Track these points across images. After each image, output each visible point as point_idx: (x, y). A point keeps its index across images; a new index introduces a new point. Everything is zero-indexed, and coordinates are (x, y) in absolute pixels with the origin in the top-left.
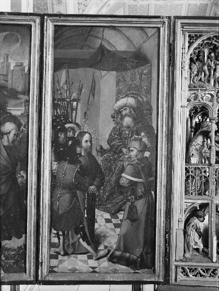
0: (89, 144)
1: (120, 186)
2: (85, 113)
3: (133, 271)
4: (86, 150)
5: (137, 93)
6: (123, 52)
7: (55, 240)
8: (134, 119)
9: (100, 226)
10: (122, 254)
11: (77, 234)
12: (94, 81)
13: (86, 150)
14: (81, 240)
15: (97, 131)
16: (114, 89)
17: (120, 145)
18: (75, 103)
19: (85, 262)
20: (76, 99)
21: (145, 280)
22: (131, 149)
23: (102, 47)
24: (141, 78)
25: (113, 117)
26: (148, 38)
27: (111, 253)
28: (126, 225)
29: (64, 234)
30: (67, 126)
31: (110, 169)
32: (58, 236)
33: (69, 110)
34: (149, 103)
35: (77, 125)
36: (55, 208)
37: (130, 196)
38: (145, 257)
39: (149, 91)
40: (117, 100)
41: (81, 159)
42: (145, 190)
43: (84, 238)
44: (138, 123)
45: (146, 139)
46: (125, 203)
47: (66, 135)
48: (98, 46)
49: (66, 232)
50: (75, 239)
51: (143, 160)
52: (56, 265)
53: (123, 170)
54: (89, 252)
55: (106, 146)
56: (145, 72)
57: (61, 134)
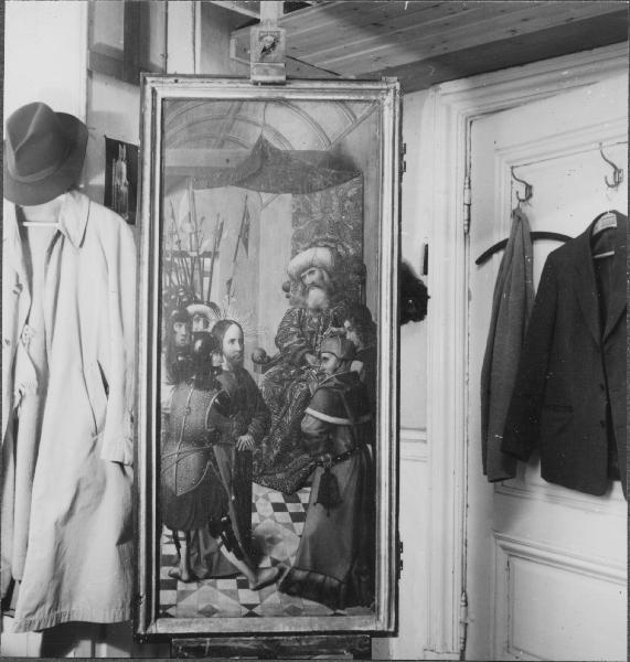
0: (237, 347)
1: (302, 435)
2: (229, 282)
3: (332, 612)
4: (230, 359)
5: (337, 238)
6: (305, 153)
7: (169, 549)
8: (331, 293)
9: (262, 518)
10: (308, 576)
11: (215, 536)
12: (246, 215)
13: (230, 359)
14: (223, 549)
15: (254, 318)
16: (290, 231)
18: (208, 261)
19: (232, 594)
20: (210, 253)
21: (356, 628)
22: (324, 355)
24: (341, 206)
25: (286, 289)
26: (357, 123)
28: (316, 515)
29: (188, 539)
30: (192, 309)
31: (281, 400)
32: (176, 541)
33: (197, 277)
34: (359, 259)
35: (212, 305)
36: (169, 480)
37: (324, 453)
38: (356, 583)
40: (295, 253)
41: (221, 378)
43: (231, 544)
44: (337, 301)
46: (312, 470)
47: (189, 329)
48: (253, 140)
49: (192, 533)
50: (212, 547)
51: (349, 378)
52: (173, 602)
53: (307, 400)
54: (240, 574)
56: (350, 194)
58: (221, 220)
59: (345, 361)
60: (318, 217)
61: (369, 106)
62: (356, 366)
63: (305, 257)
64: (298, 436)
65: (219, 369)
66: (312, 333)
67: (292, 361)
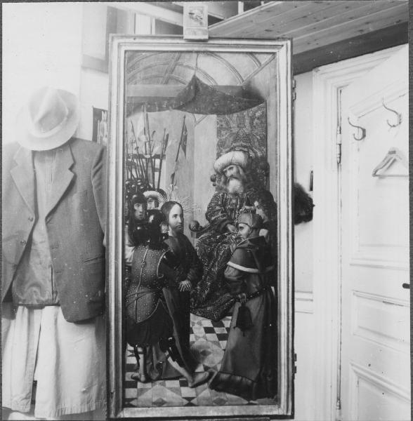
0: (179, 219)
2: (173, 176)
3: (247, 402)
4: (174, 228)
5: (248, 145)
8: (244, 183)
9: (197, 337)
10: (230, 377)
11: (164, 351)
12: (184, 129)
13: (174, 228)
14: (170, 359)
15: (190, 201)
16: (216, 140)
17: (224, 221)
19: (177, 391)
20: (159, 155)
21: (264, 413)
22: (240, 225)
23: (195, 79)
24: (251, 123)
25: (213, 180)
26: (261, 67)
27: (214, 377)
28: (235, 335)
29: (144, 352)
30: (147, 194)
31: (210, 256)
32: (136, 354)
33: (150, 172)
34: (264, 158)
35: (162, 192)
36: (131, 312)
37: (240, 293)
39: (264, 141)
40: (219, 155)
41: (168, 242)
42: (261, 283)
44: (249, 188)
45: (261, 210)
46: (232, 304)
47: (145, 207)
48: (189, 79)
49: (148, 349)
50: (162, 357)
51: (258, 241)
53: (228, 256)
55: (204, 223)
56: (258, 114)
57: (139, 206)
58: (166, 133)
59: (256, 228)
60: (235, 130)
61: (270, 56)
62: (263, 232)
63: (226, 158)
64: (222, 281)
65: (166, 235)
66: (232, 210)
67: (218, 226)
